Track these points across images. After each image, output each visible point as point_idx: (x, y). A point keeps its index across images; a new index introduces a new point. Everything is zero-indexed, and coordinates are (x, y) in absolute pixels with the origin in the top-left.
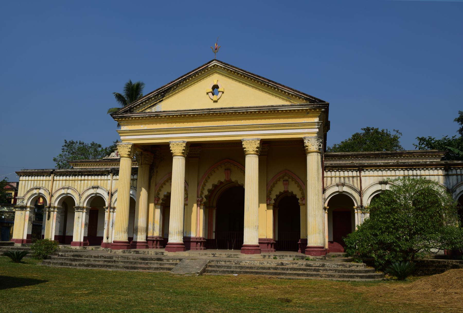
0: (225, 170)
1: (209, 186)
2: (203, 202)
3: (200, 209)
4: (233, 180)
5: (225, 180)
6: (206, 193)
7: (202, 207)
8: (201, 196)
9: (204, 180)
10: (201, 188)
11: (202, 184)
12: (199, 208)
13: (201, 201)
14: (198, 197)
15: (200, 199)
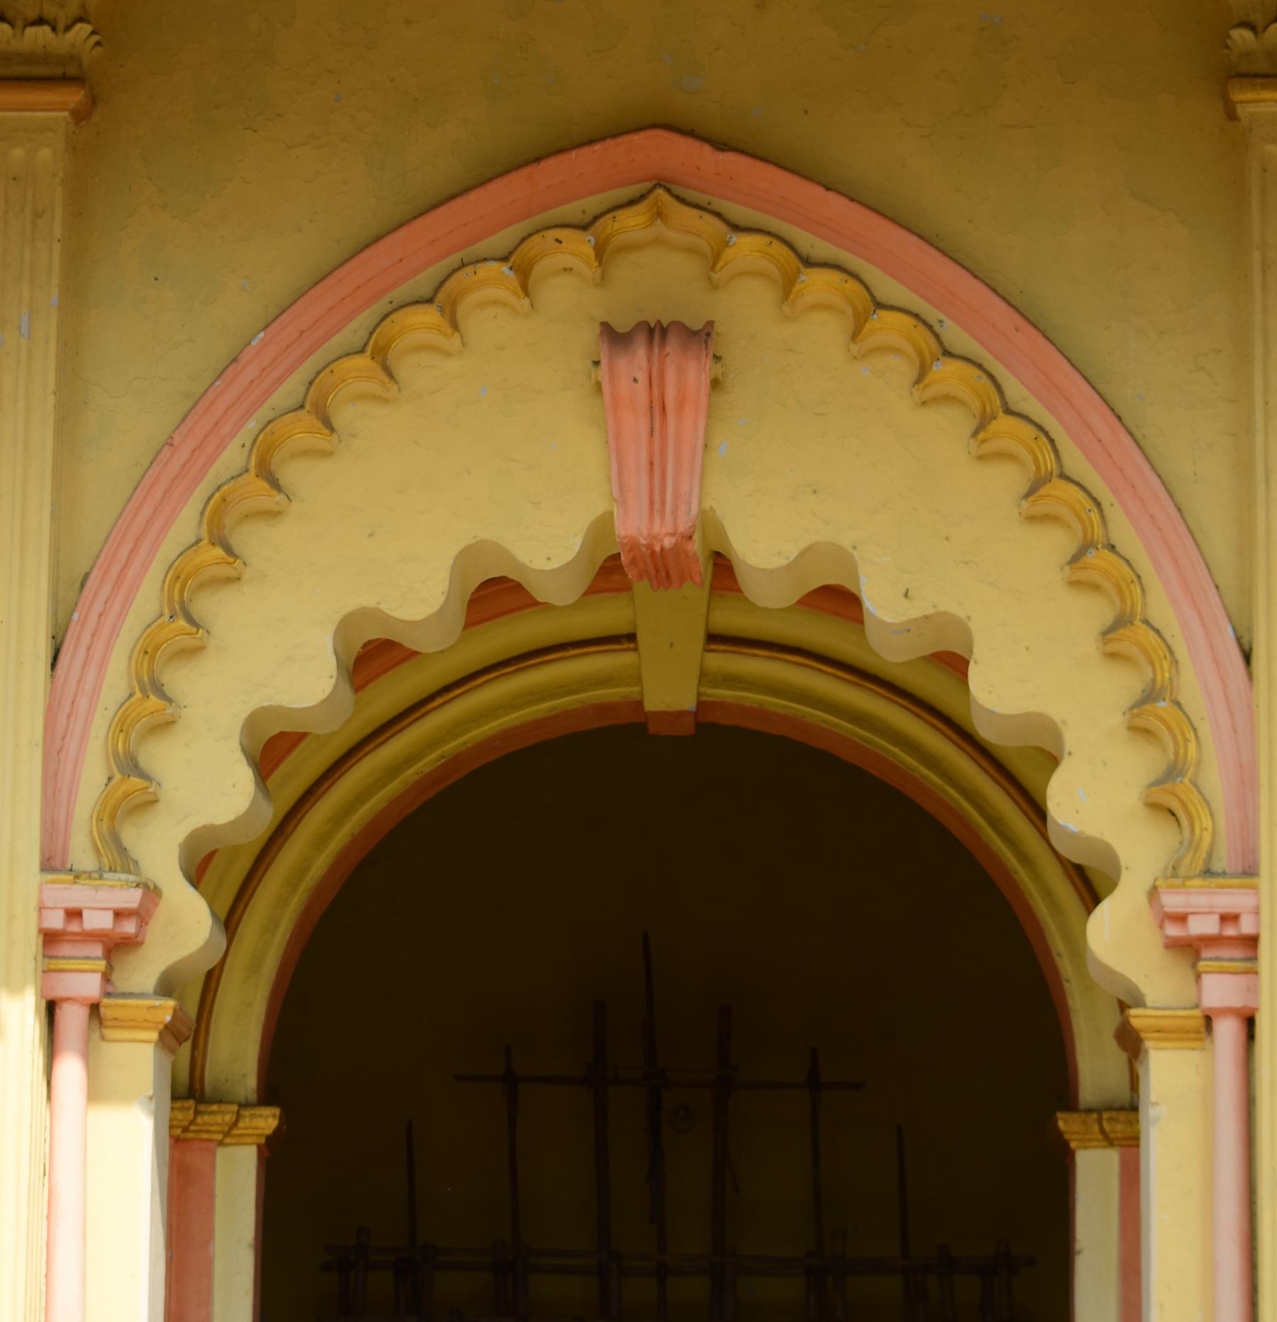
0: (616, 338)
1: (277, 653)
2: (144, 972)
3: (96, 1092)
4: (770, 541)
5: (602, 526)
6: (213, 787)
7: (139, 1059)
8: (118, 857)
9: (186, 524)
10: (116, 679)
11: (147, 600)
12: (70, 1069)
13: (117, 948)
14: (51, 863)
15: (100, 906)
